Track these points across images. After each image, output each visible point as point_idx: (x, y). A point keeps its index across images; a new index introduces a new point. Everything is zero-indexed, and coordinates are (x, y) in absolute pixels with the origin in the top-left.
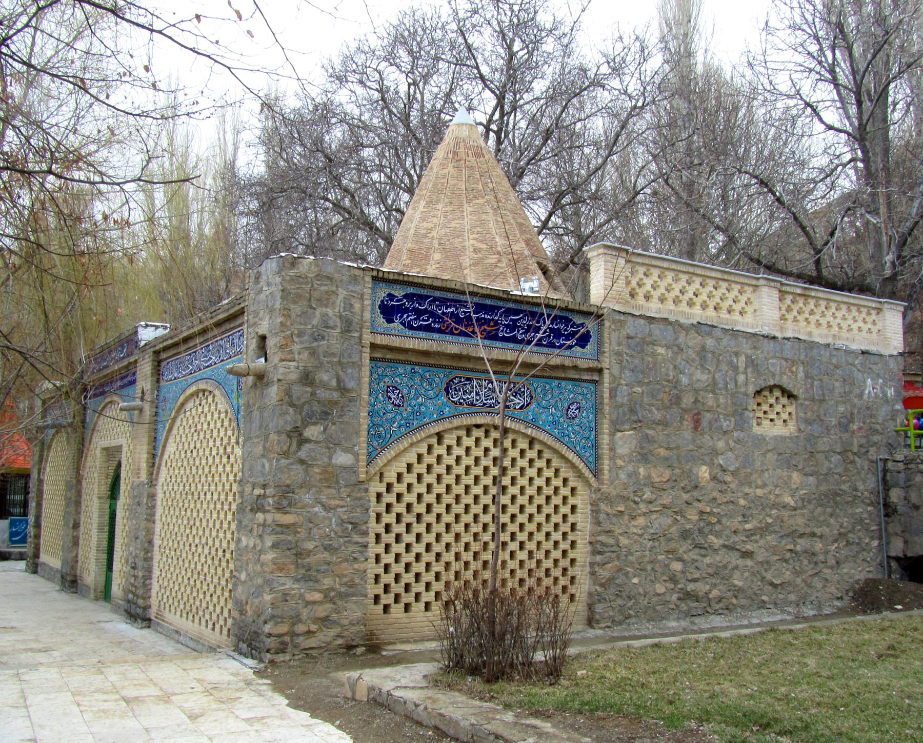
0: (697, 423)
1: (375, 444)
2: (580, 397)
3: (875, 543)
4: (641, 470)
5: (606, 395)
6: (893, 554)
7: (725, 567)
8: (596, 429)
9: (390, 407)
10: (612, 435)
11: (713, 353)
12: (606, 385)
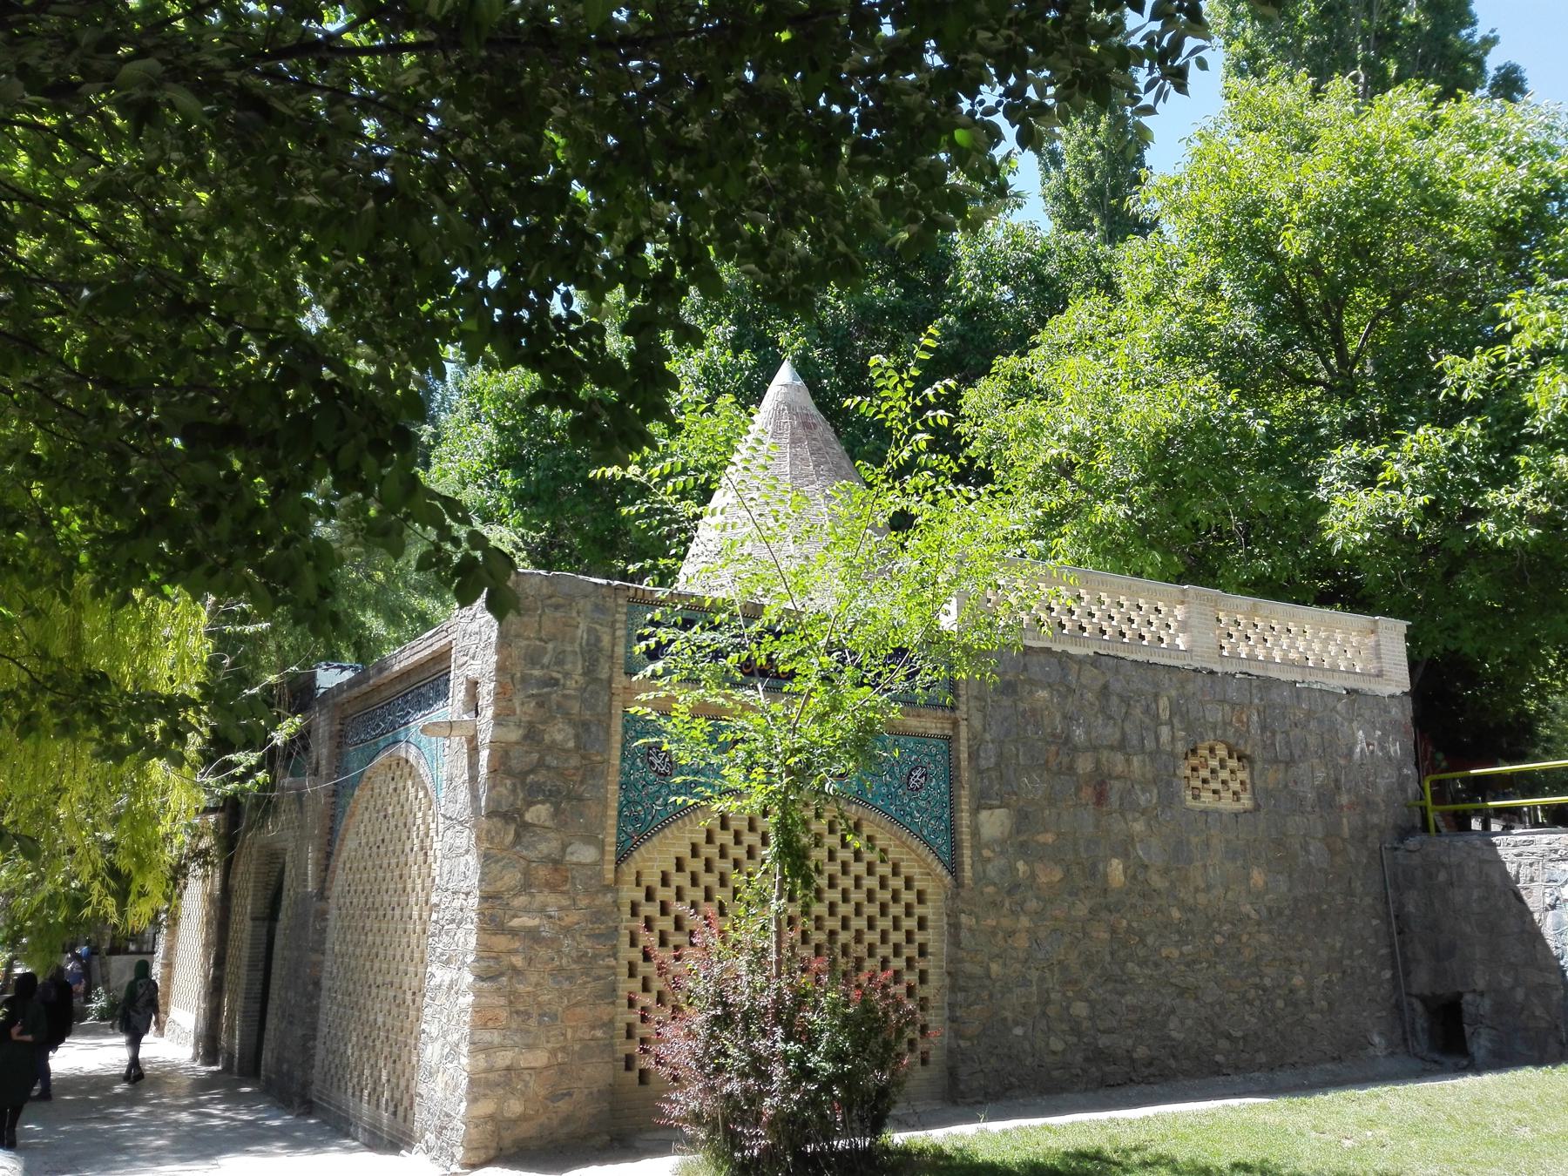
0: (1101, 797)
1: (630, 829)
2: (927, 759)
3: (1387, 974)
4: (1021, 866)
5: (964, 756)
6: (1415, 990)
7: (1157, 1009)
8: (952, 805)
9: (652, 776)
10: (975, 811)
11: (1120, 696)
12: (963, 741)
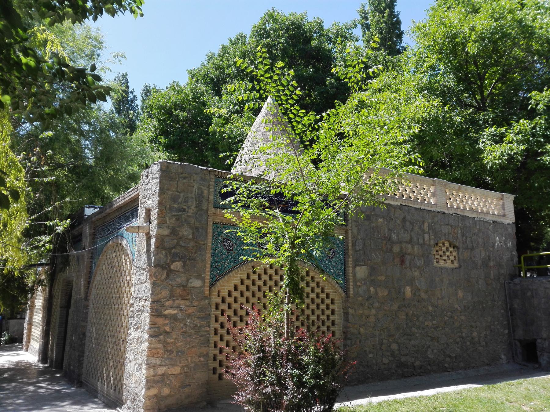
0: (402, 262)
1: (215, 273)
3: (506, 331)
4: (372, 289)
5: (350, 245)
8: (345, 265)
9: (225, 251)
10: (354, 267)
11: (410, 222)
